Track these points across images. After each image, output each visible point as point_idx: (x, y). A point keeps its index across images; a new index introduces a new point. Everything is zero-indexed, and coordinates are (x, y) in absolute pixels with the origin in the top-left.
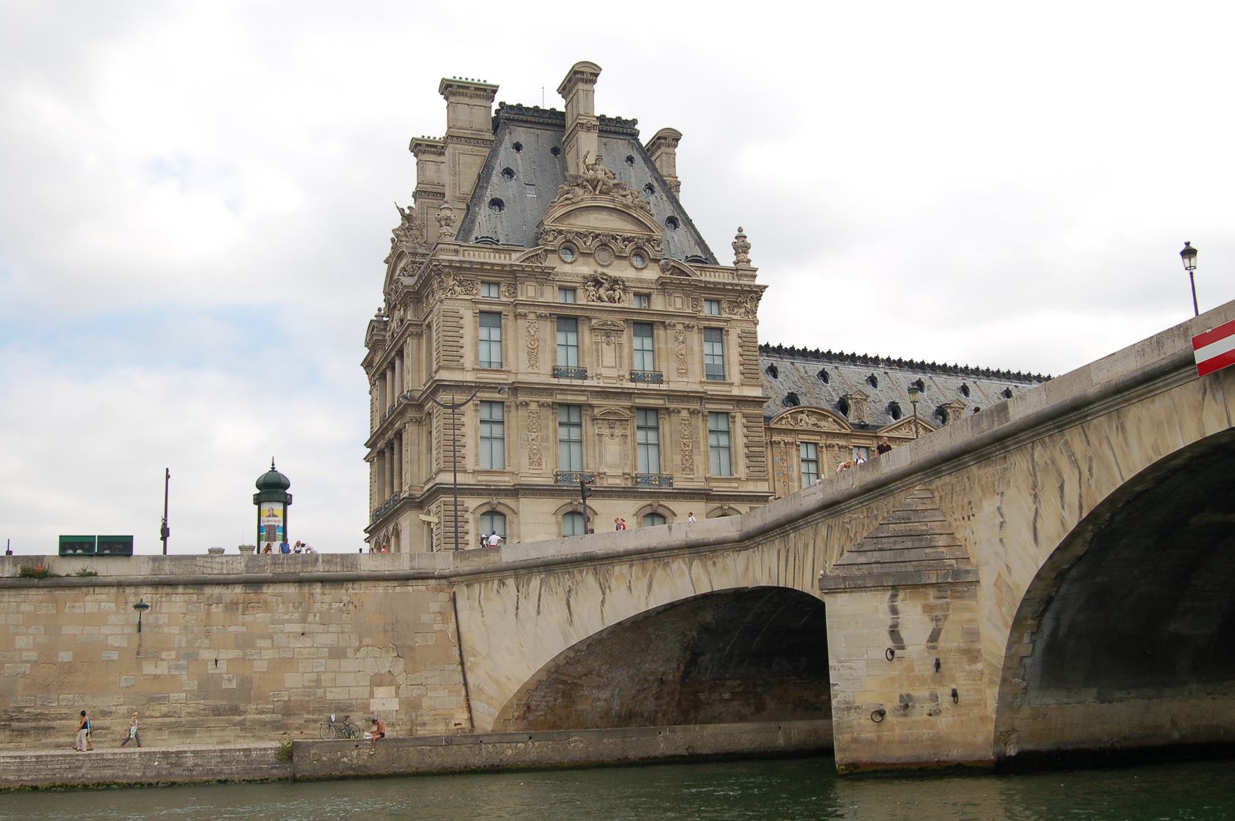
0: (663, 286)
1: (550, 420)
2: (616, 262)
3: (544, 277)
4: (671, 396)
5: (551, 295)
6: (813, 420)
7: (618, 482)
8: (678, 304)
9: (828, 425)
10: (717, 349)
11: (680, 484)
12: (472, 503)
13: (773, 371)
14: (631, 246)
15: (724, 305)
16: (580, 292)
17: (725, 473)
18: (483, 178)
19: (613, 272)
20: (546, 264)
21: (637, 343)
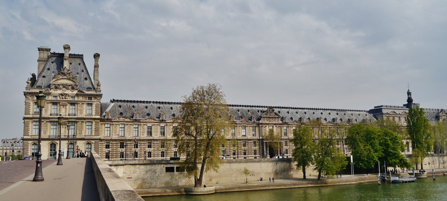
0: (77, 95)
1: (49, 124)
2: (67, 90)
3: (49, 94)
4: (77, 119)
5: (50, 98)
6: (124, 119)
7: (64, 137)
8: (81, 99)
9: (128, 120)
10: (90, 108)
11: (77, 137)
12: (30, 142)
13: (120, 106)
14: (70, 87)
15: (93, 98)
16: (58, 97)
17: (90, 134)
18: (43, 70)
19: (66, 92)
20: (50, 92)
21: (71, 107)
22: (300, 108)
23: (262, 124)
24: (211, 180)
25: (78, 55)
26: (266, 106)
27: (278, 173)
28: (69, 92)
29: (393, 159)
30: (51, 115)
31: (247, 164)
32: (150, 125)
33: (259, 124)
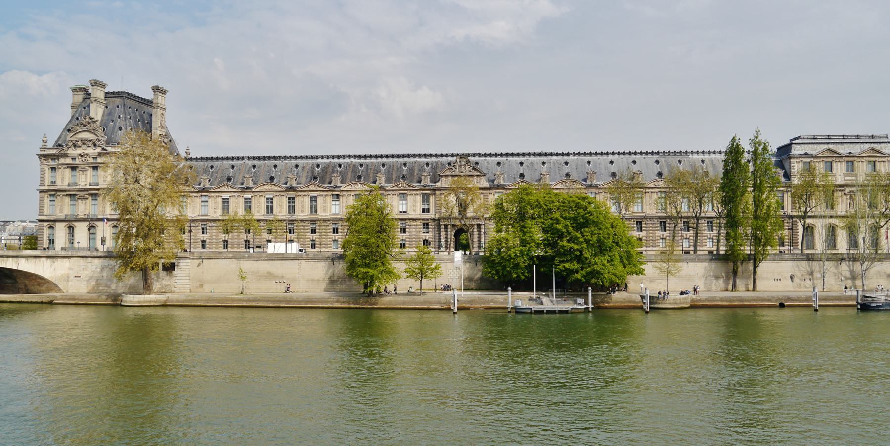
0: (100, 154)
3: (65, 155)
4: (98, 189)
5: (68, 161)
7: (83, 217)
12: (45, 224)
14: (91, 143)
22: (557, 154)
23: (439, 189)
24: (201, 286)
25: (118, 93)
26: (456, 152)
27: (336, 281)
28: (91, 151)
29: (567, 261)
30: (69, 185)
31: (271, 262)
32: (226, 196)
33: (434, 190)
